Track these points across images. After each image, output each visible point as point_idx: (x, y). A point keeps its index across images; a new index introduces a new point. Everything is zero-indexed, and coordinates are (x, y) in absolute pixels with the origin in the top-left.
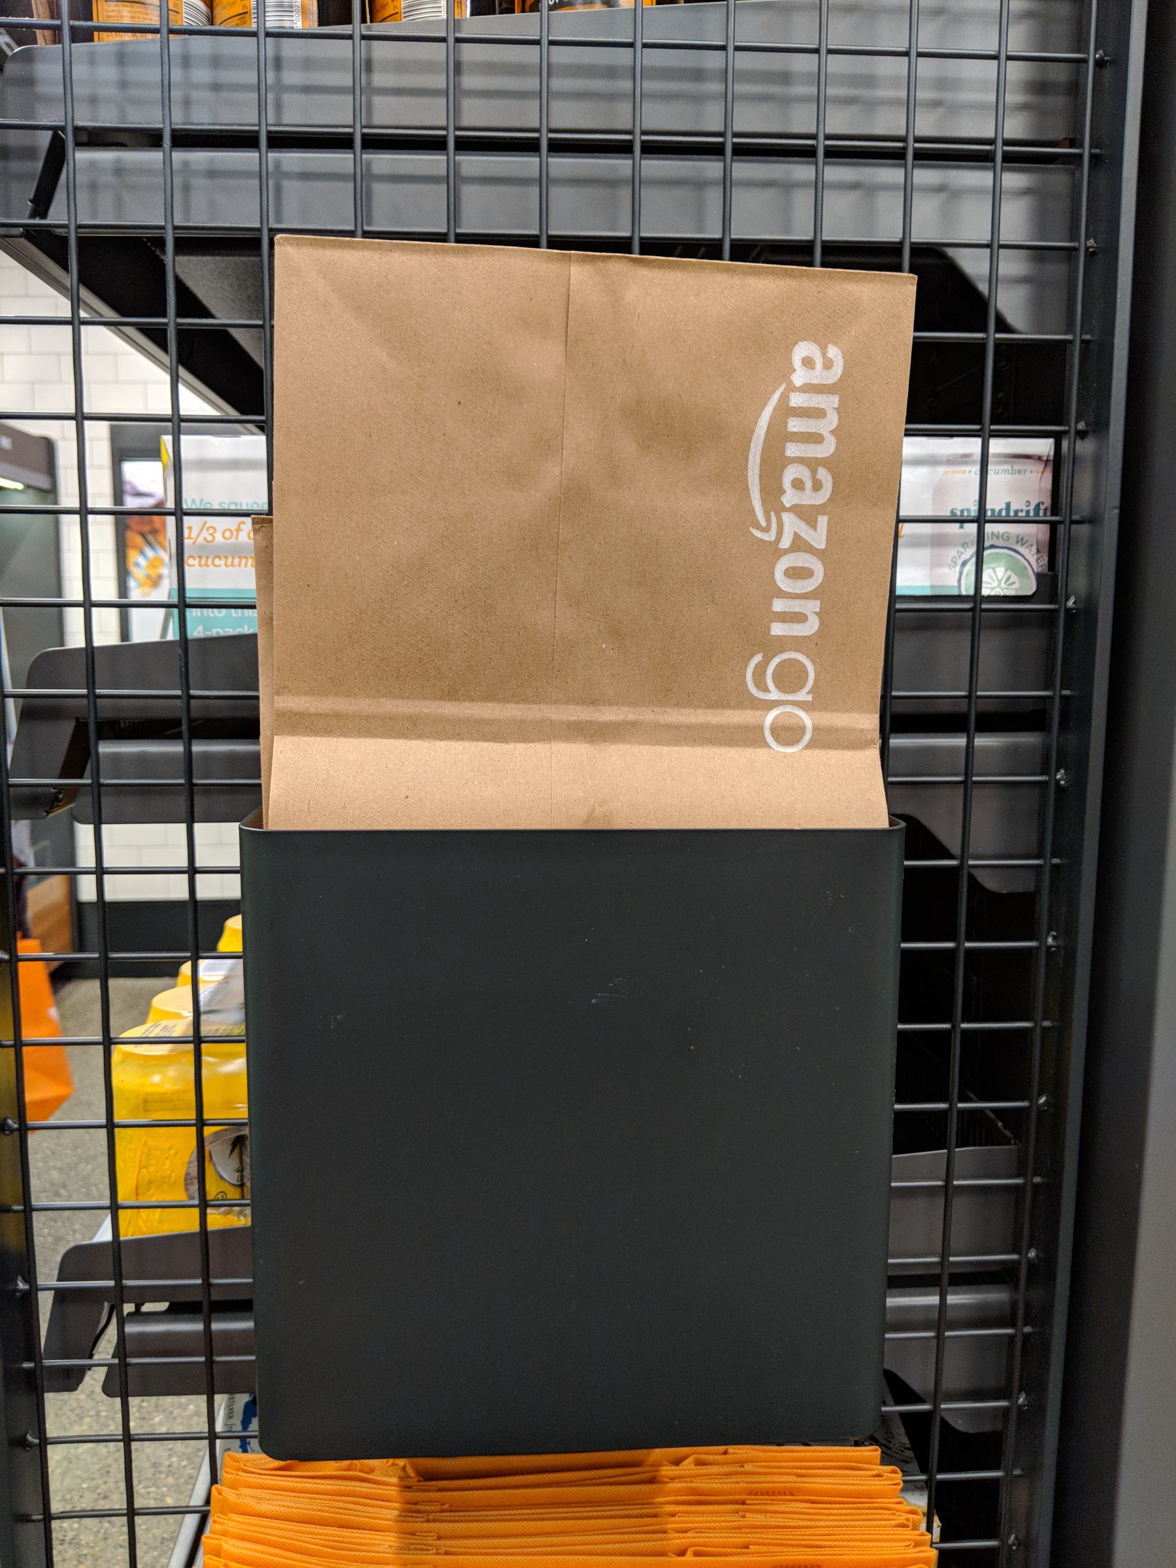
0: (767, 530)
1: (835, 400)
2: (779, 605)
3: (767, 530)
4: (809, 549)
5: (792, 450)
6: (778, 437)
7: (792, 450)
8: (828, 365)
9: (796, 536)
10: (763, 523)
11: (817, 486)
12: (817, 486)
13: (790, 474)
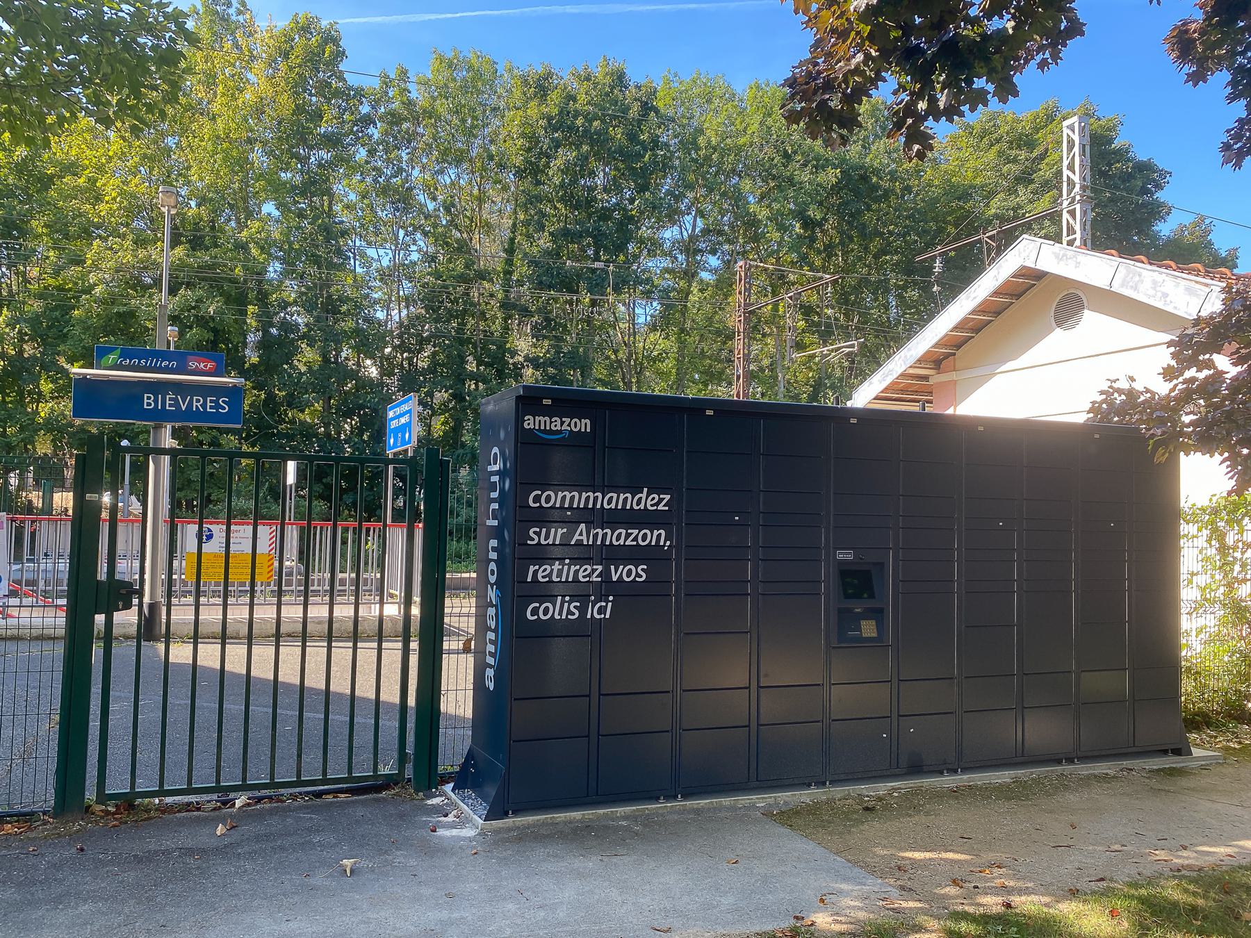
2: (583, 430)
4: (570, 423)
6: (545, 431)
7: (548, 428)
11: (556, 421)
12: (556, 421)
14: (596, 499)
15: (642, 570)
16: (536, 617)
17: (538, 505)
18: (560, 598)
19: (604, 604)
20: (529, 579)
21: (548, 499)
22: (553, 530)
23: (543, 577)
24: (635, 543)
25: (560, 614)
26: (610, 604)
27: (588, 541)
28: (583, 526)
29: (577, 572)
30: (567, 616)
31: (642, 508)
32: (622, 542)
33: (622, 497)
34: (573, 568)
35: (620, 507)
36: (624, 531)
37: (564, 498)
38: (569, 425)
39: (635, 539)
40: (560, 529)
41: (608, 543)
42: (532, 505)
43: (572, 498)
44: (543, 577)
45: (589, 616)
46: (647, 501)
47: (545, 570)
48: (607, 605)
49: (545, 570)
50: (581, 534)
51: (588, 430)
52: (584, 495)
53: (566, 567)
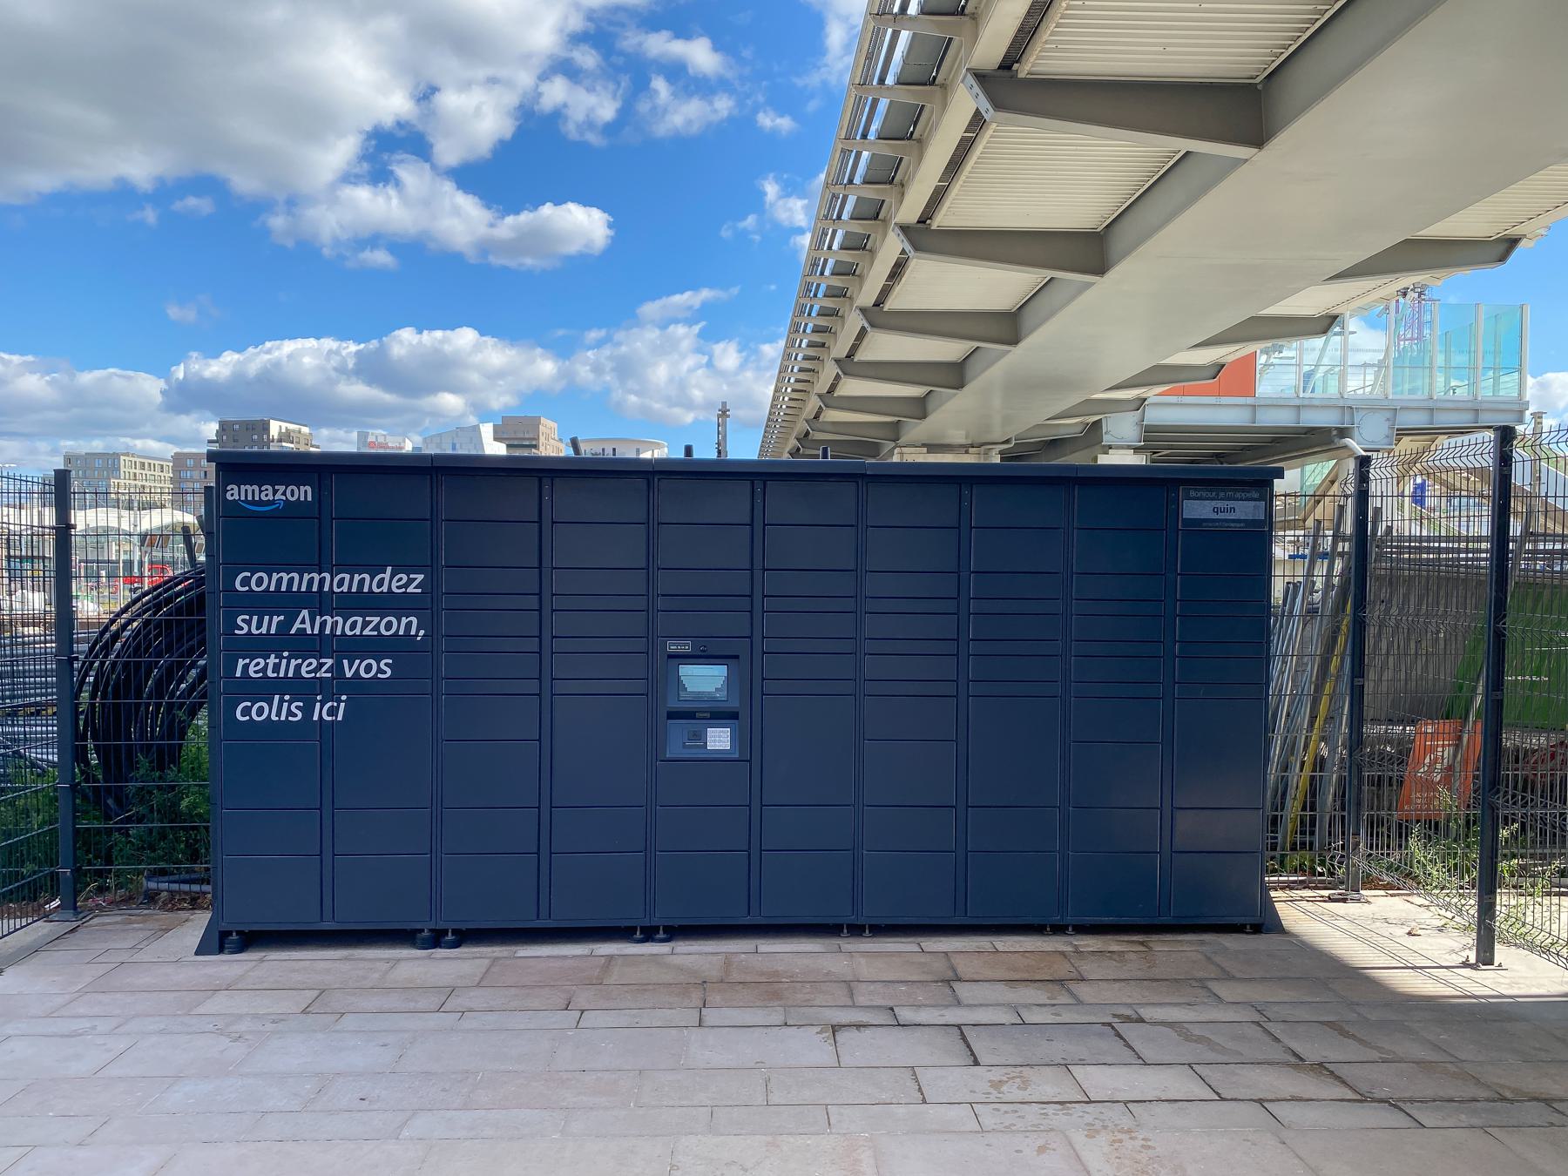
1: (242, 486)
2: (302, 499)
5: (257, 498)
6: (253, 503)
9: (282, 494)
13: (264, 498)
14: (322, 581)
15: (386, 664)
16: (248, 718)
17: (247, 588)
18: (277, 697)
19: (335, 704)
20: (238, 674)
21: (260, 582)
22: (266, 618)
23: (256, 672)
24: (376, 633)
25: (279, 714)
26: (343, 705)
27: (313, 628)
28: (305, 613)
29: (298, 667)
30: (287, 717)
31: (385, 591)
32: (357, 631)
33: (357, 578)
34: (293, 663)
35: (354, 589)
36: (360, 620)
37: (280, 581)
38: (284, 493)
39: (377, 628)
40: (275, 617)
41: (339, 633)
42: (238, 587)
43: (291, 581)
44: (256, 672)
45: (316, 718)
46: (390, 582)
47: (258, 664)
48: (339, 705)
49: (258, 664)
50: (304, 622)
51: (309, 499)
52: (306, 577)
53: (284, 661)
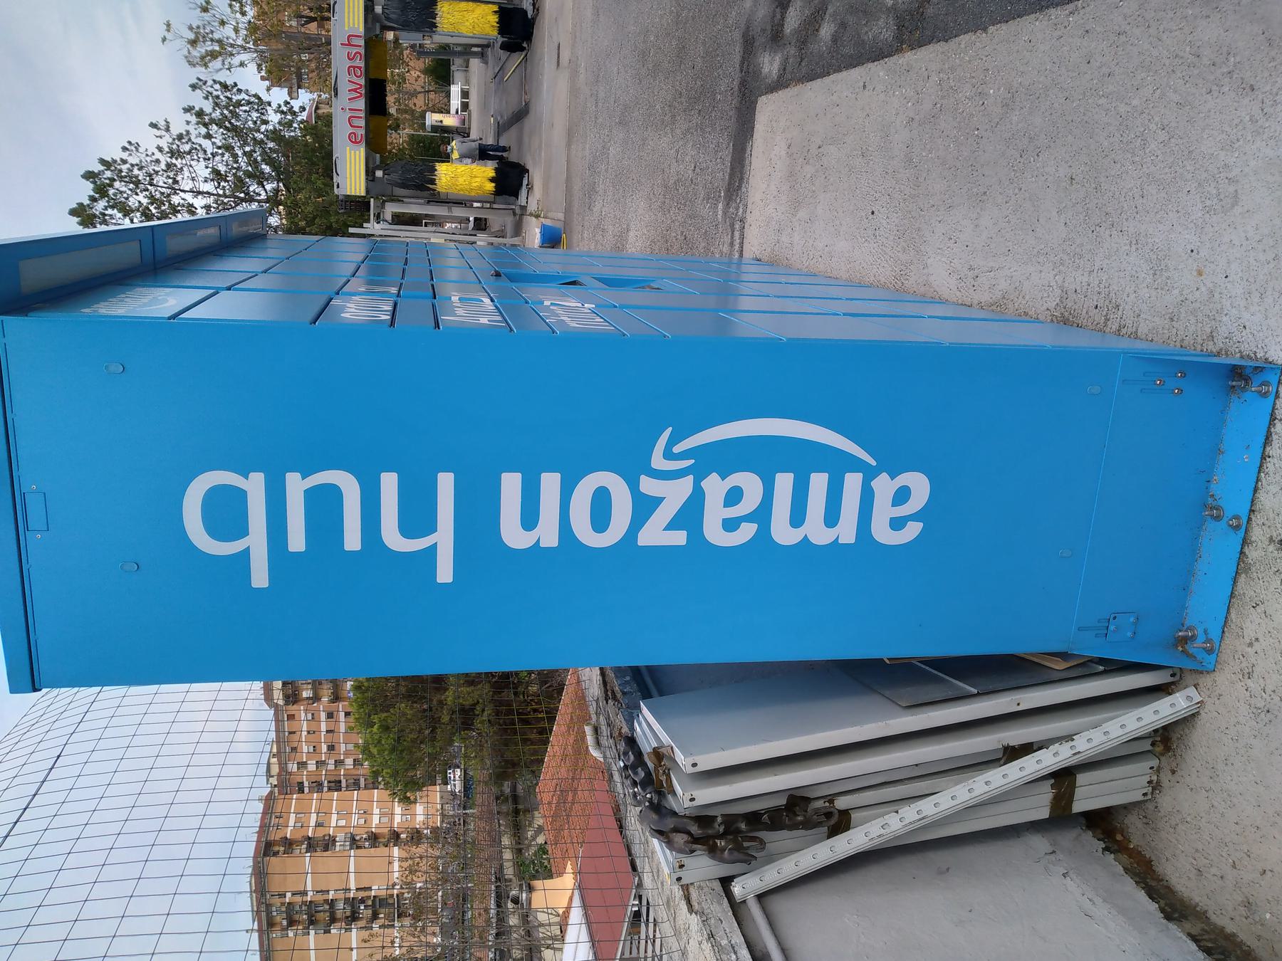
0: (668, 455)
2: (550, 483)
3: (668, 455)
5: (784, 482)
7: (784, 482)
8: (897, 524)
9: (657, 501)
10: (677, 449)
12: (730, 525)
13: (750, 483)
38: (644, 507)
51: (511, 484)
